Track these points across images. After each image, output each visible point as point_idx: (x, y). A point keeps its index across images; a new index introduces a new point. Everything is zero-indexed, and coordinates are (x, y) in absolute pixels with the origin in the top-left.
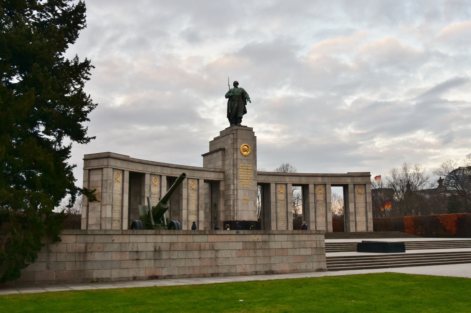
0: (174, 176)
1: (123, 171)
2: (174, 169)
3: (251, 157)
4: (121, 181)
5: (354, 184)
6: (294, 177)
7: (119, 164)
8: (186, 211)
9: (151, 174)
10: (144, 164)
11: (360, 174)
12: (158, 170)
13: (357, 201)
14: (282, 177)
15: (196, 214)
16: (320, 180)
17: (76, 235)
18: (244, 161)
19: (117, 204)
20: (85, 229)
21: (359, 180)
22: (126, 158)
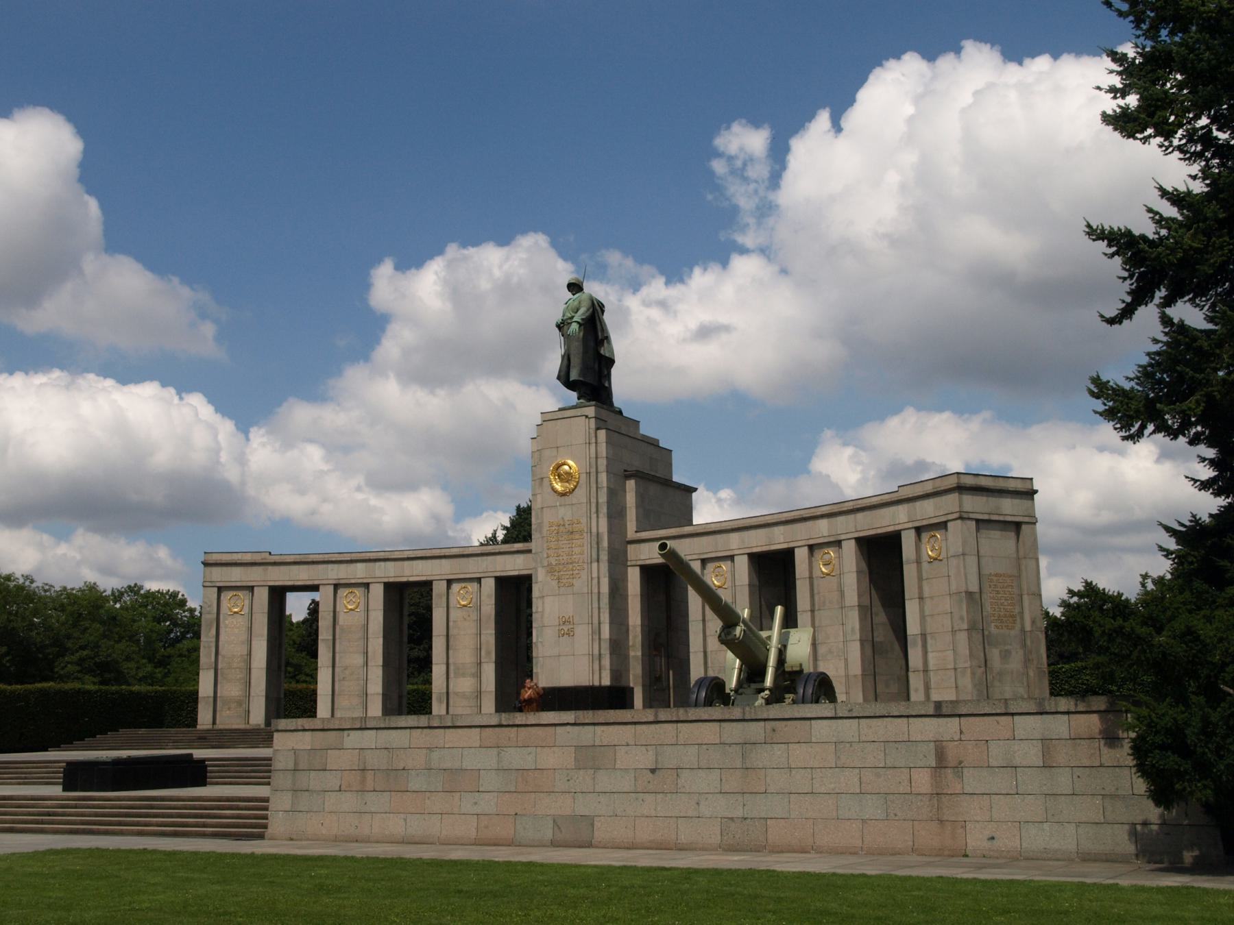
0: (405, 579)
1: (253, 587)
2: (406, 563)
3: (581, 494)
4: (246, 610)
5: (919, 530)
6: (752, 533)
7: (236, 576)
8: (444, 667)
9: (336, 587)
10: (313, 563)
11: (929, 488)
12: (359, 572)
13: (927, 591)
14: (718, 536)
15: (473, 675)
16: (822, 529)
17: (1068, 713)
18: (562, 511)
19: (235, 665)
20: (328, 715)
21: (928, 511)
22: (257, 558)
